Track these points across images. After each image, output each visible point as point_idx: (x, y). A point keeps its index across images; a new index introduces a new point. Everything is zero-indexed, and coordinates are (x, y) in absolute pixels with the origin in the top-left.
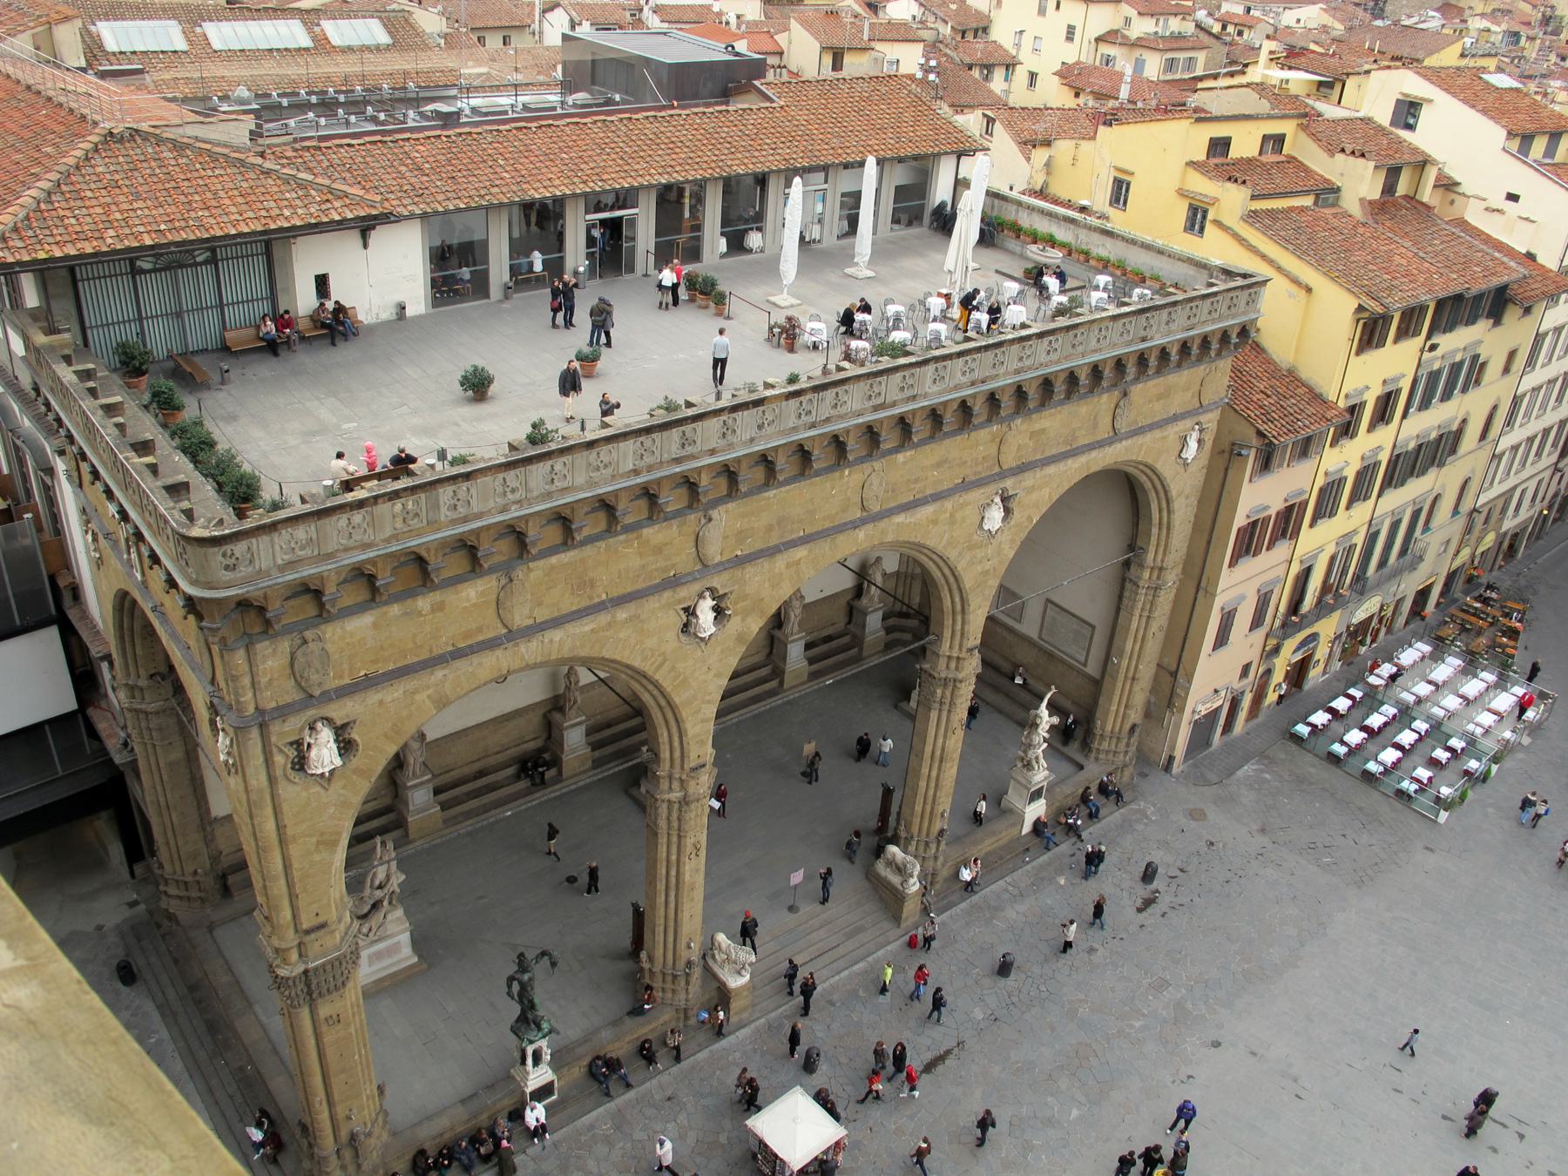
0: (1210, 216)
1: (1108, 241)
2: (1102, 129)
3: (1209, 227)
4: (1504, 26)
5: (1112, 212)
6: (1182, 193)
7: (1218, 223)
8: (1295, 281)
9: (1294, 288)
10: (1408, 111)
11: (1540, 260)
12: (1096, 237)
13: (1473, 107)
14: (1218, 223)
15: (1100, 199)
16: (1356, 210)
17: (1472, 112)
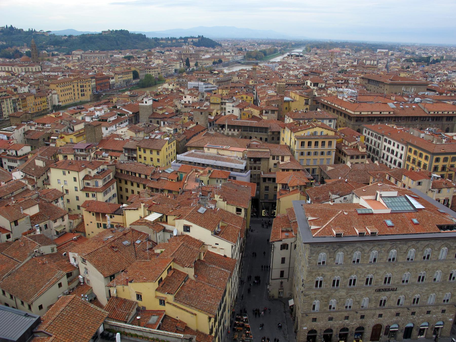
0: (166, 301)
1: (152, 335)
2: (129, 284)
3: (166, 304)
4: (173, 128)
5: (138, 301)
6: (156, 297)
7: (168, 303)
8: (192, 314)
9: (192, 315)
10: (187, 228)
11: (227, 256)
12: (148, 334)
13: (202, 226)
14: (168, 303)
15: (134, 299)
16: (193, 278)
17: (202, 228)
